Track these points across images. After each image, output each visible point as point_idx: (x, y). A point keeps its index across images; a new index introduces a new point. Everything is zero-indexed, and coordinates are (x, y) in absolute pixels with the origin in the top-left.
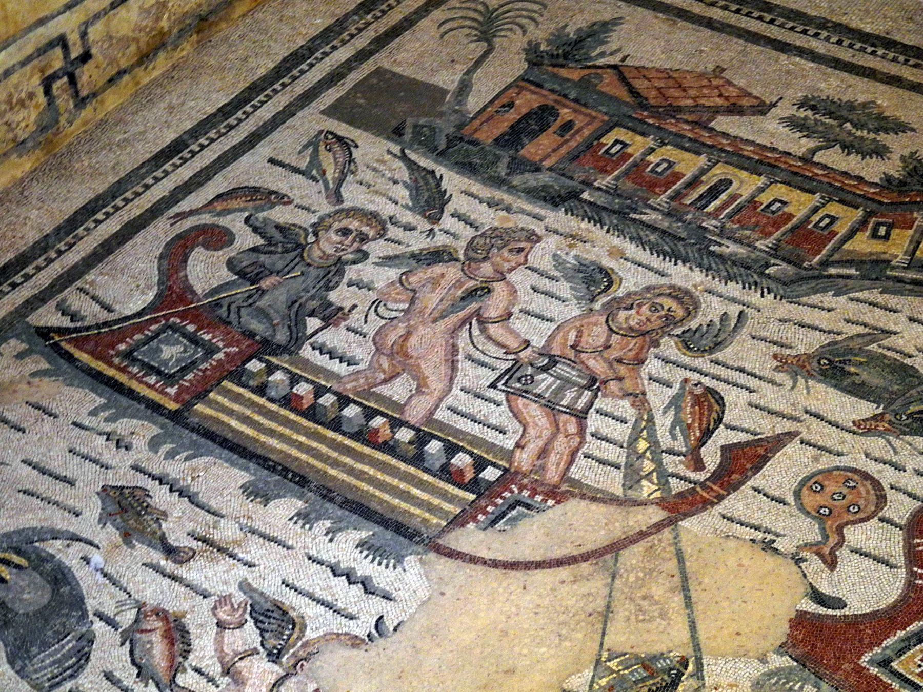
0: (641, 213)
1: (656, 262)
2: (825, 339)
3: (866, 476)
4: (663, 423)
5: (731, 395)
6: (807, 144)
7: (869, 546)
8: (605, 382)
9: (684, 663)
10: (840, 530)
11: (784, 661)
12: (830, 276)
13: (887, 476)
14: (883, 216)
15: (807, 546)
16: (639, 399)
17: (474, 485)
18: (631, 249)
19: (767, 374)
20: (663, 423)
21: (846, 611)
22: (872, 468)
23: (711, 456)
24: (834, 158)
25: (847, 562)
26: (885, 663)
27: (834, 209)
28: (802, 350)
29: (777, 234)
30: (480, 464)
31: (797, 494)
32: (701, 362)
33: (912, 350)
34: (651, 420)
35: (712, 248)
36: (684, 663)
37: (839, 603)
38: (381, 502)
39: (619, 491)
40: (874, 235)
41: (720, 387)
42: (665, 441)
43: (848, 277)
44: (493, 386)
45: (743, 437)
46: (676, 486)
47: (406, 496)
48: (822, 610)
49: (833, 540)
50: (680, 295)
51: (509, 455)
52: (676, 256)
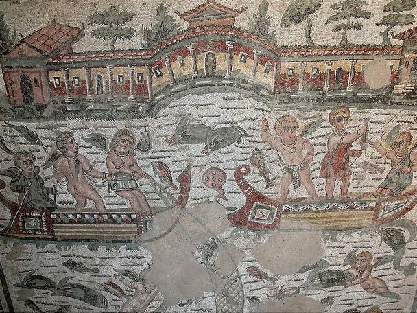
0: (89, 106)
1: (109, 124)
2: (174, 127)
3: (217, 169)
4: (157, 179)
5: (167, 161)
6: (110, 41)
7: (231, 190)
8: (134, 175)
9: (213, 239)
10: (221, 188)
11: (233, 229)
12: (159, 101)
13: (221, 166)
14: (154, 65)
15: (217, 197)
16: (148, 177)
17: (133, 221)
18: (99, 123)
19: (168, 149)
20: (157, 179)
21: (237, 210)
22: (215, 166)
23: (177, 184)
24: (120, 45)
25: (228, 196)
26: (254, 218)
27: (138, 70)
28: (171, 135)
29: (131, 93)
30: (129, 215)
31: (205, 183)
32: (150, 154)
33: (198, 119)
34: (154, 181)
35: (119, 108)
36: (213, 239)
37: (235, 209)
38: (119, 237)
39: (164, 206)
40: (158, 76)
41: (161, 160)
42: (164, 186)
43: (163, 99)
44: (110, 192)
45: (180, 173)
46: (177, 197)
47: (124, 233)
48: (232, 212)
49: (221, 192)
50: (125, 133)
51: (132, 209)
52: (111, 118)
